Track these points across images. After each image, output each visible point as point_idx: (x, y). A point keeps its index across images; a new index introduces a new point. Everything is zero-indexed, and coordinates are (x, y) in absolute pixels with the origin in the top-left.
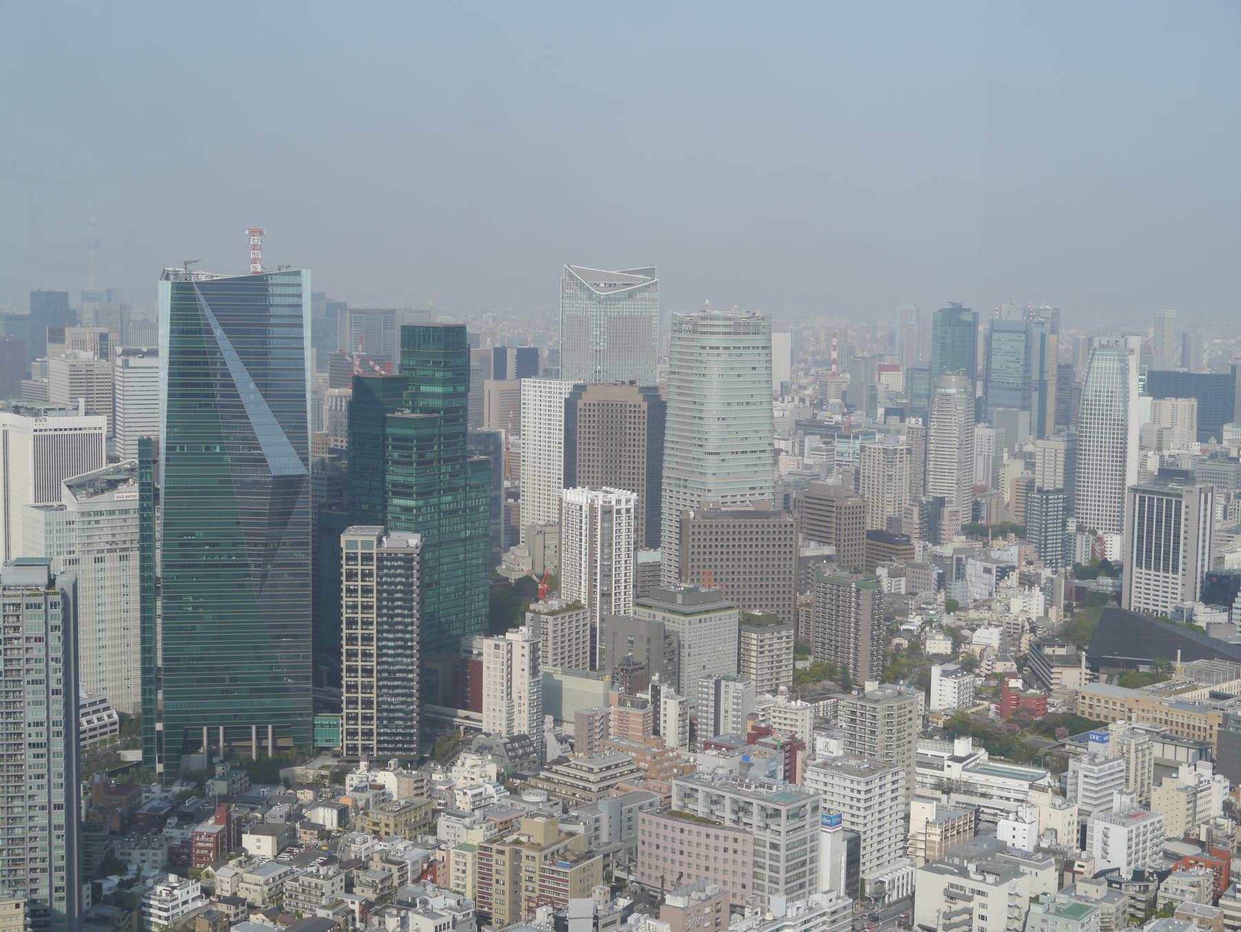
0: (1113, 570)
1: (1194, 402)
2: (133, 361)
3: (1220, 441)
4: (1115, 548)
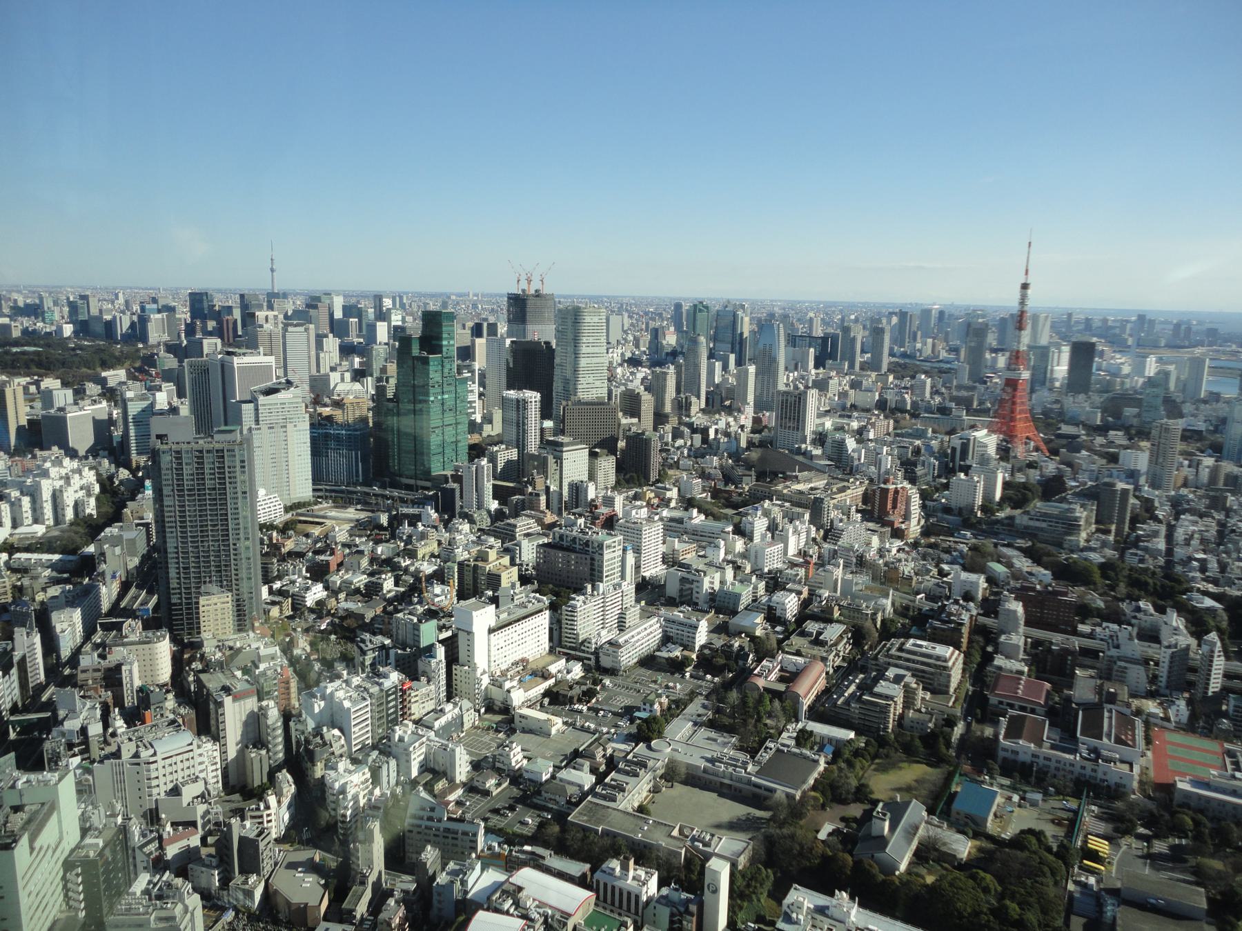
2: (290, 329)
4: (770, 418)
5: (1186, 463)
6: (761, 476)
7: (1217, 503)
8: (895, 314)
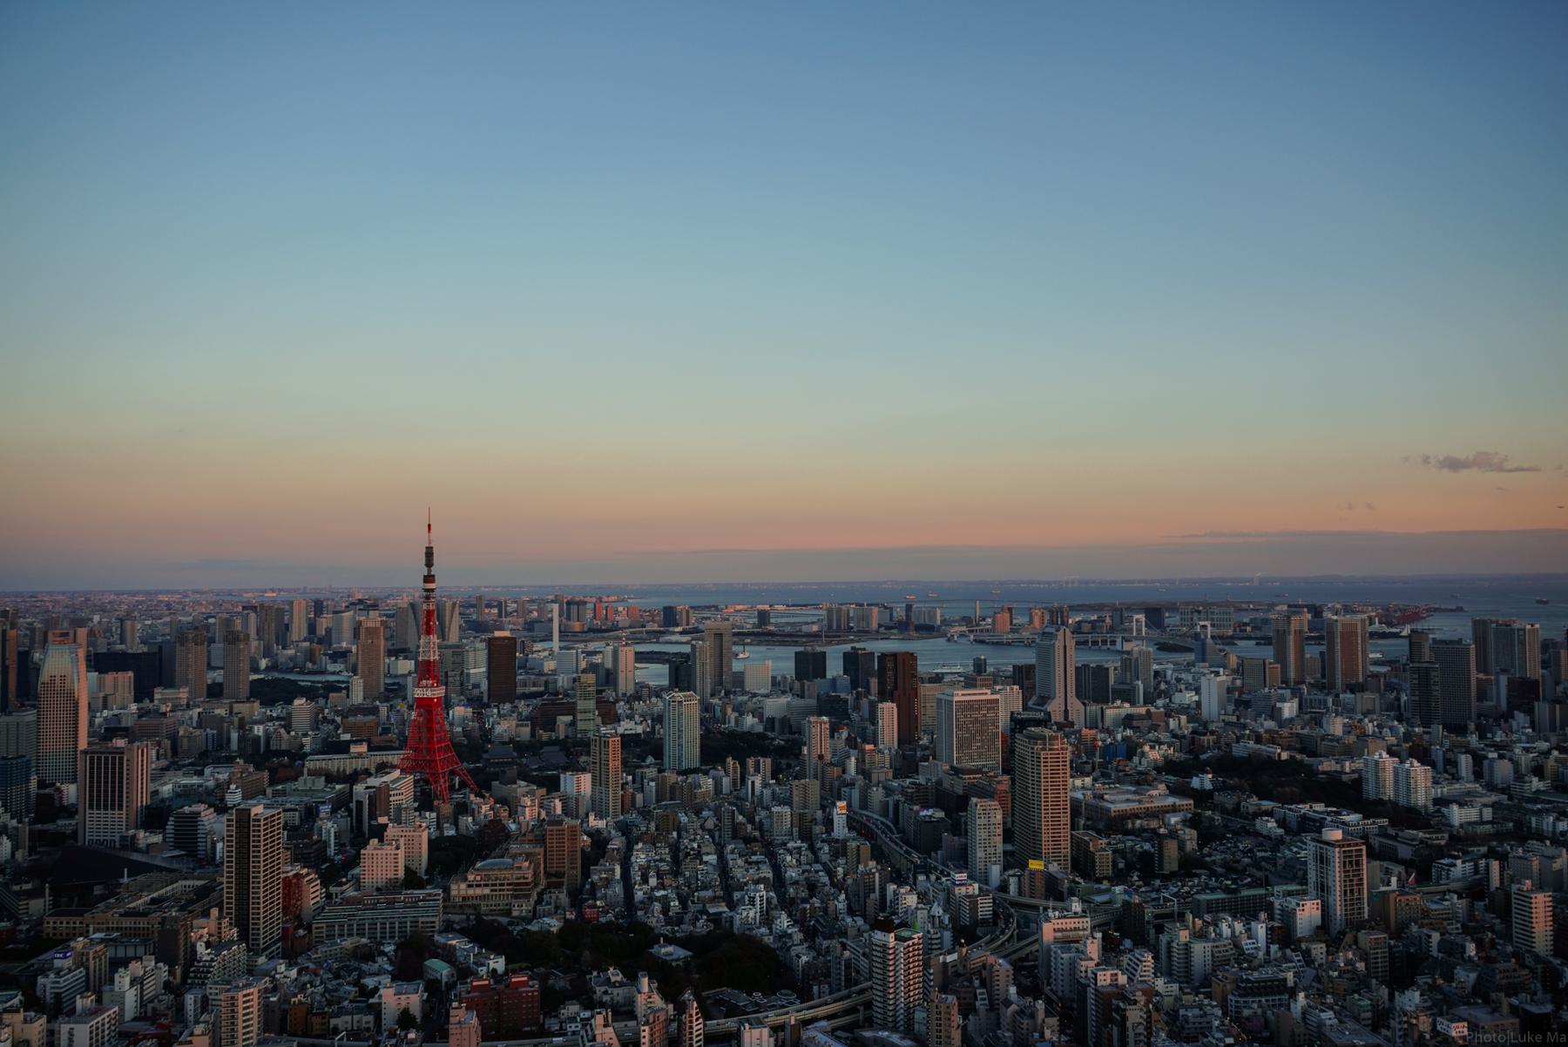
0: (70, 811)
1: (131, 674)
3: (152, 701)
4: (70, 791)
6: (56, 893)
7: (667, 824)
8: (254, 608)
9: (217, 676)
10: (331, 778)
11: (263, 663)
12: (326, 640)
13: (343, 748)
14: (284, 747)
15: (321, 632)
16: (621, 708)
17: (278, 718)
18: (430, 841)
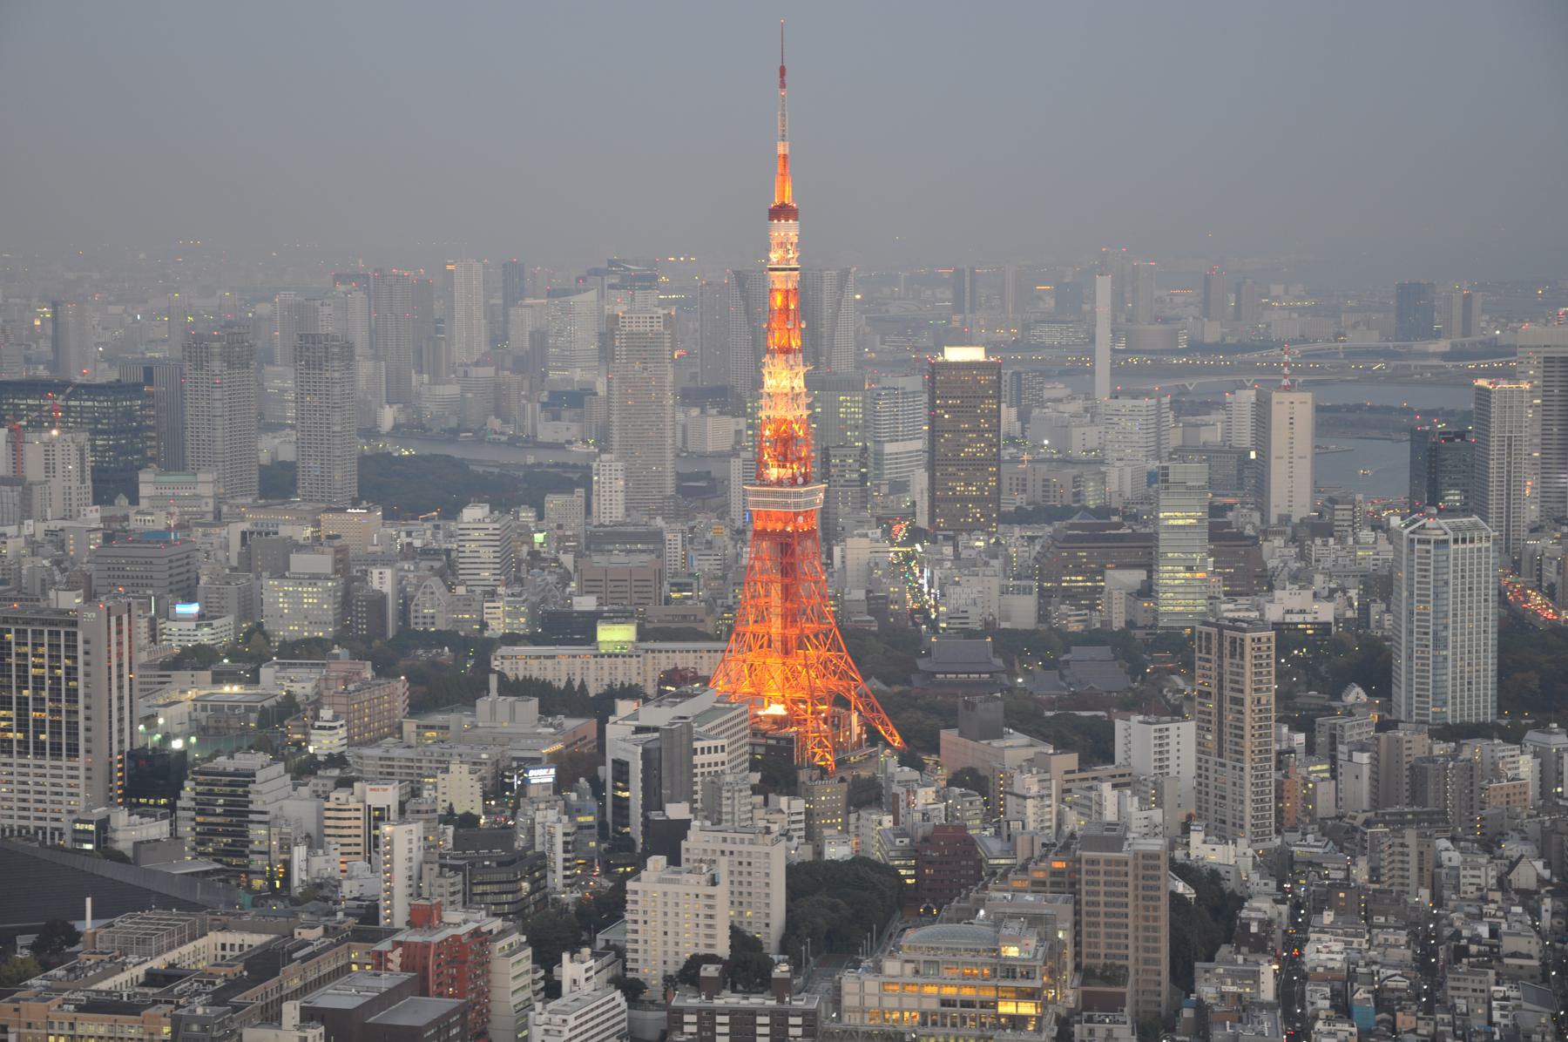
3: (134, 500)
5: (1300, 738)
9: (276, 447)
10: (555, 700)
11: (388, 417)
12: (532, 362)
13: (580, 630)
14: (441, 625)
15: (520, 340)
16: (1276, 552)
17: (426, 552)
18: (792, 871)
